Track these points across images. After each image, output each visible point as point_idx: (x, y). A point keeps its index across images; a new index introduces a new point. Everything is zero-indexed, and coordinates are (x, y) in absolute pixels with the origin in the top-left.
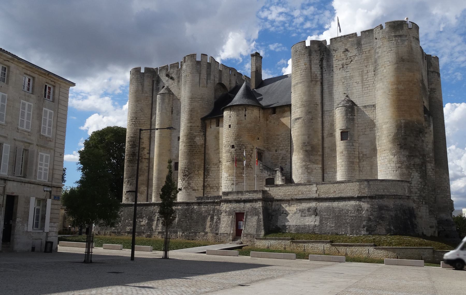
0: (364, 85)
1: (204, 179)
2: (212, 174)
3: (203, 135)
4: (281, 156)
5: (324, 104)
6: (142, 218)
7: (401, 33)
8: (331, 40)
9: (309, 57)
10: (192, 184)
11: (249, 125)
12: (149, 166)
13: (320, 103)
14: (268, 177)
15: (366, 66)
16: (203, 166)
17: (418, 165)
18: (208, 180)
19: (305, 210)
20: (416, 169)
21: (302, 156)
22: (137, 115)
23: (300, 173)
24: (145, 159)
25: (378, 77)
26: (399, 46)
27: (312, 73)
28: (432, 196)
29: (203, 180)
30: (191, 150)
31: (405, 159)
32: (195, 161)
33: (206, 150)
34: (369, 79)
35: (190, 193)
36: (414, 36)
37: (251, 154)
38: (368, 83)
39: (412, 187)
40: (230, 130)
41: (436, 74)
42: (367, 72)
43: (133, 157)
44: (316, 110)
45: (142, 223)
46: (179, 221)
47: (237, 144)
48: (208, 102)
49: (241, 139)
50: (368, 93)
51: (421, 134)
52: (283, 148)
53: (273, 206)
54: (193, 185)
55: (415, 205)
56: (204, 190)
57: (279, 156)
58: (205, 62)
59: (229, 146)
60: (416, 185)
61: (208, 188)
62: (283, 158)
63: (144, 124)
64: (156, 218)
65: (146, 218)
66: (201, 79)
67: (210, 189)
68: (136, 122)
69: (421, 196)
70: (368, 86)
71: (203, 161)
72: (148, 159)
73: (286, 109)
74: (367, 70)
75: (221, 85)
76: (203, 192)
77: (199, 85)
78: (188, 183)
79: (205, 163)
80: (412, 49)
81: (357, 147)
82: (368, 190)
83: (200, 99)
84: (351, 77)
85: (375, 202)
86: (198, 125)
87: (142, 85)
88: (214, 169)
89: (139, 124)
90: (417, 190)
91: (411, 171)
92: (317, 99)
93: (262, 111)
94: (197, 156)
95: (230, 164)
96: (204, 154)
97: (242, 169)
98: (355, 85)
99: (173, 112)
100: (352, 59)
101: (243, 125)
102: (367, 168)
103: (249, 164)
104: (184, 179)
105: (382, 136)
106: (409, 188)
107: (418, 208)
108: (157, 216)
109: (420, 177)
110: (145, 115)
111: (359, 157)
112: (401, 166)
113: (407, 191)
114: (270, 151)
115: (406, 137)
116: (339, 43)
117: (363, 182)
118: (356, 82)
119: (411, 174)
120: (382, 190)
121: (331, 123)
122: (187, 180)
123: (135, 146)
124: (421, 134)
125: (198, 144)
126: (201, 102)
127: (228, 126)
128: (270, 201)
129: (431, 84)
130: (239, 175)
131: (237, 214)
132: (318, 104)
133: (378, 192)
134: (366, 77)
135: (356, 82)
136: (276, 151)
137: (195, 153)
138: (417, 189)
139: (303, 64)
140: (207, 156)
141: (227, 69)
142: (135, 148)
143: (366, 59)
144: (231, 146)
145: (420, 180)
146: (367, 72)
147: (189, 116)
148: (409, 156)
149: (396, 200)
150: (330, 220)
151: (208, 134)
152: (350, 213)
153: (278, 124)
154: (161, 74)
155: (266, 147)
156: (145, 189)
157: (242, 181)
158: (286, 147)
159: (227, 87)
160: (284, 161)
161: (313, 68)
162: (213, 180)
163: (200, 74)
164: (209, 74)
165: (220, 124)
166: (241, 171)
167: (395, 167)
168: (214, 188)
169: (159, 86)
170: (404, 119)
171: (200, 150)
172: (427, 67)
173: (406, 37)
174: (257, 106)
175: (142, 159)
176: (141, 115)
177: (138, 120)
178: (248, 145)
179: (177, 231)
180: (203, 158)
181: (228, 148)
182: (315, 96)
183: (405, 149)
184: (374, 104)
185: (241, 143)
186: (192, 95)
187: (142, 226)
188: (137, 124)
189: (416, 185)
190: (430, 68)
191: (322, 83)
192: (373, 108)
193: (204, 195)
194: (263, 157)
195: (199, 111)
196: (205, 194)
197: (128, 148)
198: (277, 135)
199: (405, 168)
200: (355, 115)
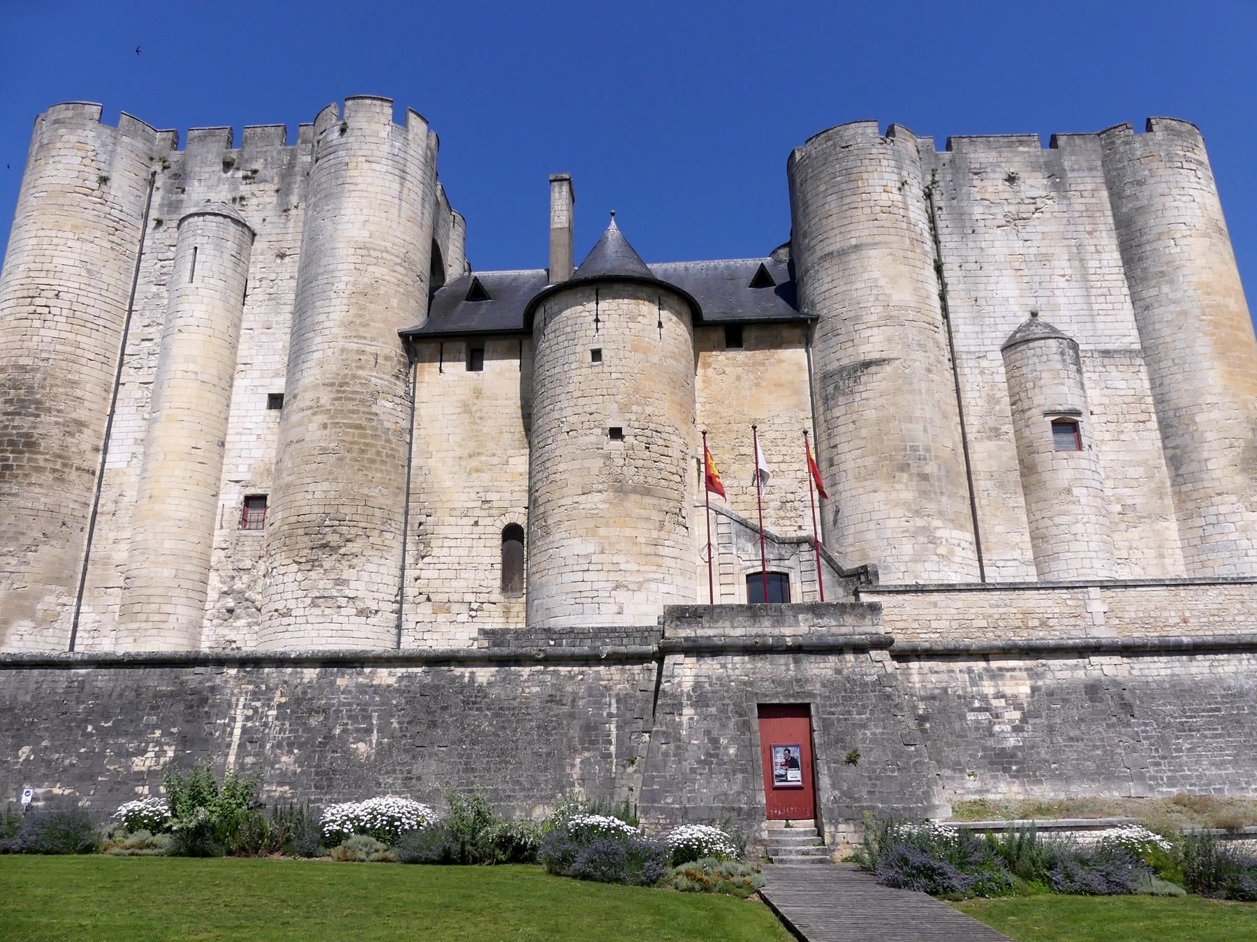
2: (445, 551)
10: (353, 584)
15: (1090, 233)
18: (424, 574)
22: (62, 283)
24: (78, 469)
30: (357, 443)
35: (345, 627)
43: (22, 452)
47: (636, 424)
50: (1109, 312)
52: (784, 467)
54: (357, 588)
59: (599, 431)
63: (95, 327)
64: (237, 732)
70: (1104, 291)
84: (1044, 259)
86: (387, 351)
89: (70, 320)
94: (381, 471)
97: (657, 525)
98: (1061, 282)
100: (1039, 205)
102: (1146, 551)
108: (239, 725)
118: (1064, 276)
122: (334, 568)
130: (650, 549)
134: (1097, 264)
135: (1064, 276)
137: (372, 461)
147: (353, 312)
151: (422, 393)
157: (657, 576)
162: (451, 574)
166: (655, 534)
171: (392, 449)
176: (83, 286)
185: (652, 426)
188: (56, 318)
195: (394, 302)
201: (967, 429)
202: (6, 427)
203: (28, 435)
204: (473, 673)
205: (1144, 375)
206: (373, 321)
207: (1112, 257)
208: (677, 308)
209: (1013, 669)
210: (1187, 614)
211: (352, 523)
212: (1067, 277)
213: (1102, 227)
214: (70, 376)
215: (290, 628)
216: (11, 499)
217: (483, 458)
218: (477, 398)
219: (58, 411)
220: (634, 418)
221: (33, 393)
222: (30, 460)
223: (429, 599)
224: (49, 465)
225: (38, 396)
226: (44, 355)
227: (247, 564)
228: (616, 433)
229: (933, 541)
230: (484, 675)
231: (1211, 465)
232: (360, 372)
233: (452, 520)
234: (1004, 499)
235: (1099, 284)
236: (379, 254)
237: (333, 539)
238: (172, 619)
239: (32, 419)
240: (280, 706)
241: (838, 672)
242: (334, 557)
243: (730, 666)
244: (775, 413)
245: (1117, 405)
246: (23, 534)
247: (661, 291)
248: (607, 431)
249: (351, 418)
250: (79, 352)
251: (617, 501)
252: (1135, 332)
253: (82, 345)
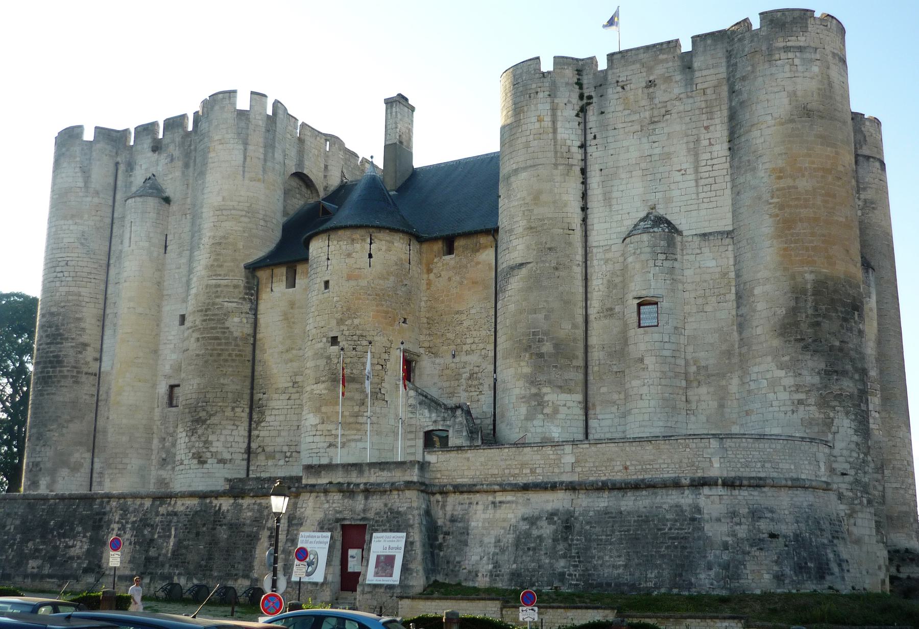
0: (701, 178)
1: (250, 431)
2: (273, 417)
3: (250, 309)
4: (467, 369)
5: (589, 227)
6: (74, 537)
7: (802, 41)
8: (611, 57)
9: (549, 100)
10: (215, 444)
11: (381, 282)
12: (98, 396)
13: (579, 225)
14: (431, 428)
15: (707, 128)
16: (247, 397)
17: (851, 396)
18: (262, 434)
19: (539, 518)
20: (844, 407)
21: (527, 370)
23: (523, 418)
24: (86, 373)
25: (740, 158)
26: (796, 75)
27: (559, 142)
28: (877, 484)
29: (246, 434)
30: (216, 350)
31: (816, 380)
32: (226, 381)
33: (257, 352)
34: (715, 161)
35: (211, 471)
36: (836, 51)
37: (382, 362)
38: (713, 174)
39: (835, 457)
40: (326, 295)
41: (877, 164)
42: (710, 142)
43: (55, 367)
44: (570, 244)
45: (73, 552)
46: (179, 545)
47: (347, 333)
48: (265, 221)
49: (356, 321)
51: (856, 313)
52: (474, 347)
53: (449, 508)
54: (217, 446)
55: (842, 507)
56: (248, 460)
57: (462, 370)
58: (260, 114)
59: (324, 340)
60: (845, 453)
61: (261, 457)
62: (472, 375)
63: (89, 280)
65: (84, 537)
66: (248, 159)
67: (267, 459)
68: (66, 274)
69: (857, 481)
70: (711, 180)
71: (248, 383)
72: (95, 375)
73: (484, 240)
74: (710, 139)
75: (301, 177)
76: (245, 468)
77: (241, 173)
78: (206, 442)
79: (252, 388)
80: (830, 84)
81: (683, 346)
82: (721, 463)
83: (244, 213)
84: (666, 157)
85: (739, 497)
86: (235, 282)
87: (86, 173)
88: (279, 402)
89: (75, 279)
90: (847, 466)
91: (832, 415)
92: (569, 215)
93: (415, 246)
95: (326, 389)
96: (250, 364)
98: (677, 177)
99: (168, 248)
100: (669, 108)
101: (363, 283)
103: (378, 390)
104: (193, 432)
105: (752, 316)
106: (831, 458)
109: (856, 431)
110: (92, 256)
111: (686, 374)
112: (806, 399)
113: (823, 469)
114: (436, 355)
115: (819, 319)
116: (633, 67)
117: (707, 440)
119: (833, 420)
120: (759, 465)
121: (609, 281)
122: (203, 434)
123: (61, 339)
124: (856, 313)
125: (236, 334)
126: (246, 220)
127: (323, 285)
128: (441, 493)
129: (865, 189)
130: (352, 420)
131: (344, 527)
132: (574, 227)
133: (748, 469)
134: (708, 156)
136: (454, 356)
137: (226, 361)
138: (849, 463)
139: (534, 119)
140: (258, 368)
141: (318, 138)
142: (62, 343)
143: (706, 108)
144: (327, 338)
145: (855, 438)
146: (711, 144)
147: (212, 258)
148: (825, 371)
149: (796, 492)
150: (611, 550)
151: (262, 307)
152: (670, 529)
153: (461, 283)
154: (139, 147)
155: (426, 344)
156: (85, 458)
157: (356, 437)
158: (481, 346)
159: (317, 187)
160: (475, 383)
161: (559, 130)
162: (274, 433)
163: (246, 144)
164: (269, 146)
165: (297, 281)
166: (356, 409)
167: (789, 403)
168: (277, 456)
169: (132, 179)
170: (812, 272)
171: (240, 351)
172: (855, 145)
173: (815, 52)
174: (403, 232)
175: (80, 375)
177: (72, 269)
178: (376, 338)
179: (170, 573)
180: (248, 372)
181: (320, 345)
182: (565, 205)
183: (815, 351)
184: (730, 228)
185: (358, 332)
186: (223, 201)
187: (71, 558)
188: (67, 279)
189: (845, 453)
190: (861, 147)
191: (583, 171)
192: (728, 241)
193: (248, 474)
194: (417, 372)
195: (240, 245)
196: (251, 472)
197: (40, 345)
198: (457, 312)
199: (815, 405)
200: (676, 260)
201: (590, 311)
202: (47, 352)
203: (57, 356)
204: (221, 504)
205: (730, 254)
206: (225, 262)
207: (721, 149)
208: (388, 238)
209: (508, 502)
210: (628, 463)
211: (214, 404)
212: (683, 172)
213: (717, 121)
214: (77, 316)
215: (183, 472)
216: (52, 396)
217: (294, 352)
218: (292, 308)
219: (73, 339)
220: (346, 328)
221: (59, 329)
222: (60, 371)
223: (264, 450)
224: (69, 374)
225: (61, 331)
226: (62, 304)
227: (171, 430)
228: (334, 341)
229: (541, 404)
230: (225, 504)
231: (759, 331)
232: (217, 300)
233: (276, 396)
234: (610, 365)
235: (707, 175)
236: (229, 213)
237: (203, 414)
238: (129, 467)
239: (59, 346)
240: (134, 523)
241: (386, 505)
242: (204, 426)
243: (331, 501)
244: (471, 305)
245: (706, 281)
246: (60, 417)
247: (371, 230)
248: (330, 339)
249: (212, 333)
250: (81, 298)
251: (332, 388)
252: (730, 215)
253: (82, 294)
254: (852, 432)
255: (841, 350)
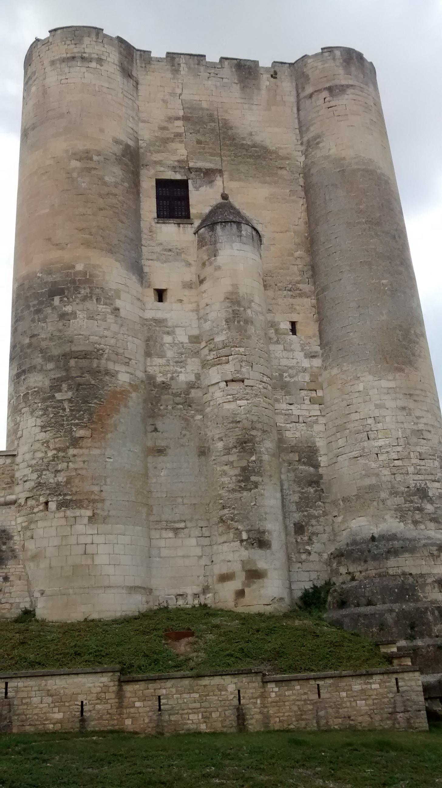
107: (26, 528)
109: (42, 427)
129: (308, 129)
138: (31, 466)
254: (38, 429)
255: (30, 345)
